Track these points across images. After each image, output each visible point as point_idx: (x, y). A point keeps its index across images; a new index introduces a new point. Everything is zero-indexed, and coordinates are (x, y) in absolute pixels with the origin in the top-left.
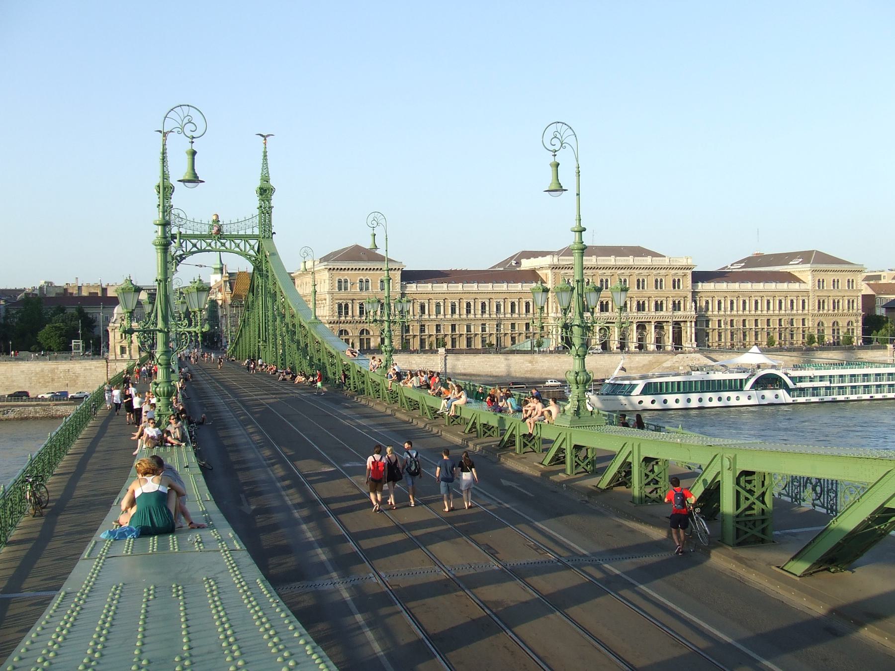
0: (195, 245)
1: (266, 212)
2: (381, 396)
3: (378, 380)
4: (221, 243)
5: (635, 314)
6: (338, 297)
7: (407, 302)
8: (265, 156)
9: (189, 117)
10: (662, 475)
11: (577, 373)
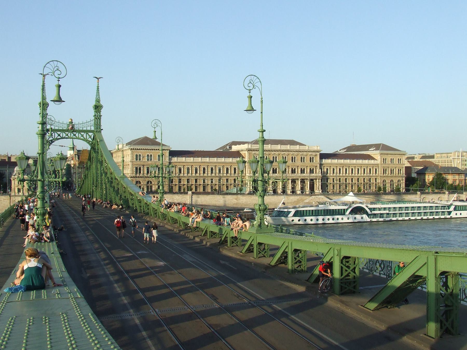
0: (59, 135)
1: (98, 118)
2: (158, 216)
3: (156, 208)
4: (74, 134)
5: (291, 175)
6: (136, 164)
7: (172, 167)
8: (98, 89)
9: (58, 67)
10: (303, 258)
11: (260, 205)
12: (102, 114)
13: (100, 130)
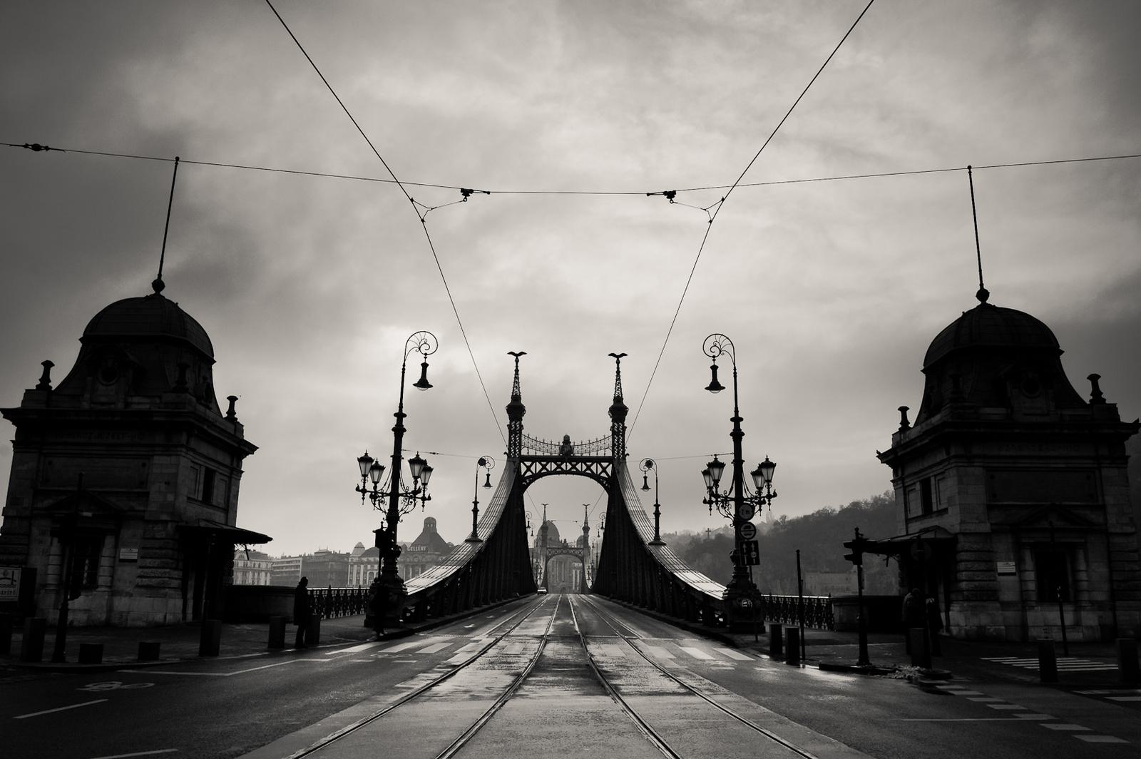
0: (544, 467)
1: (618, 432)
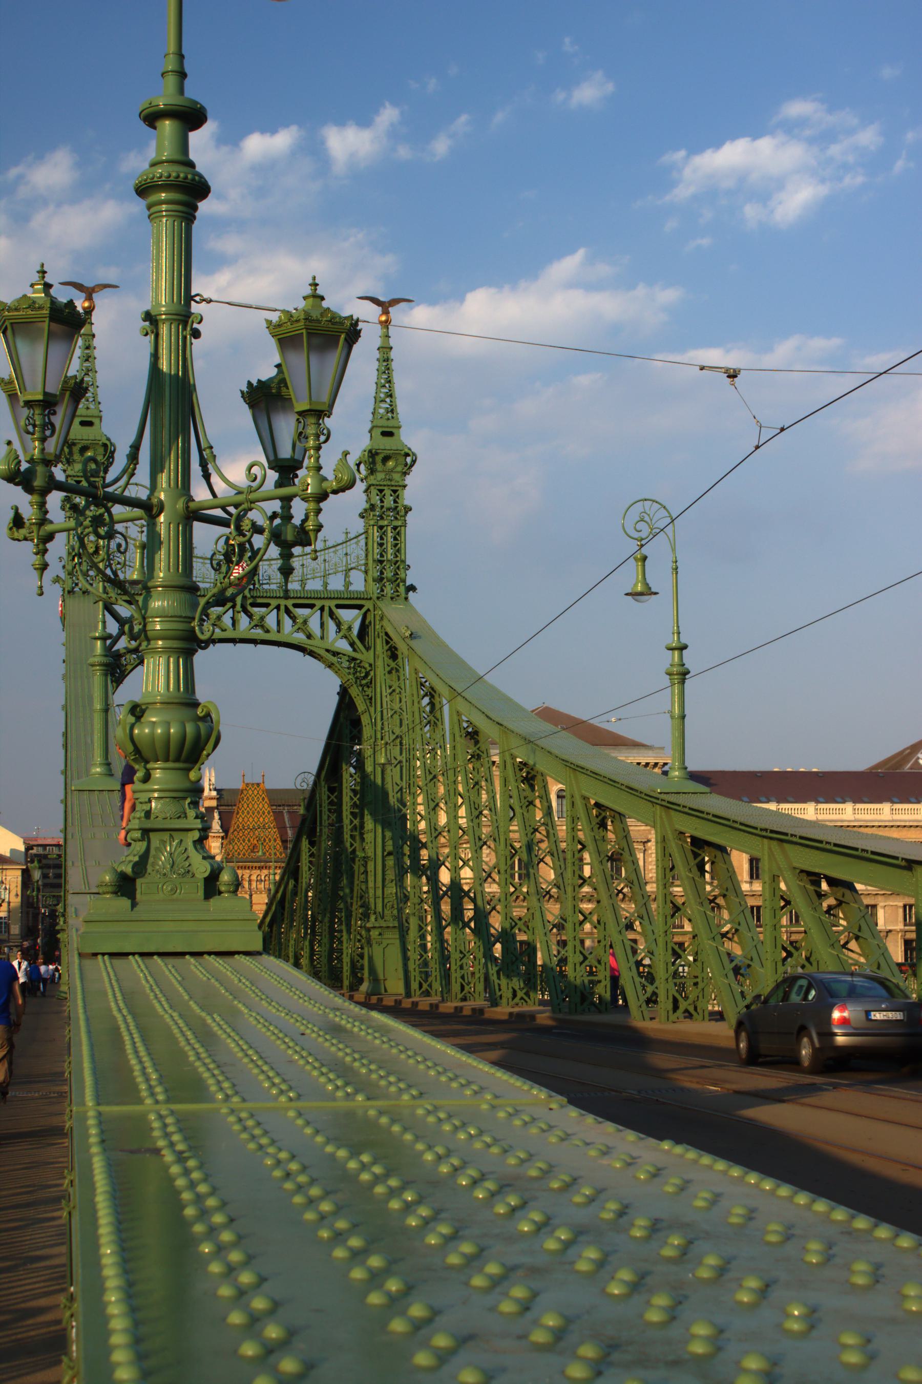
12: (408, 497)
13: (402, 589)
